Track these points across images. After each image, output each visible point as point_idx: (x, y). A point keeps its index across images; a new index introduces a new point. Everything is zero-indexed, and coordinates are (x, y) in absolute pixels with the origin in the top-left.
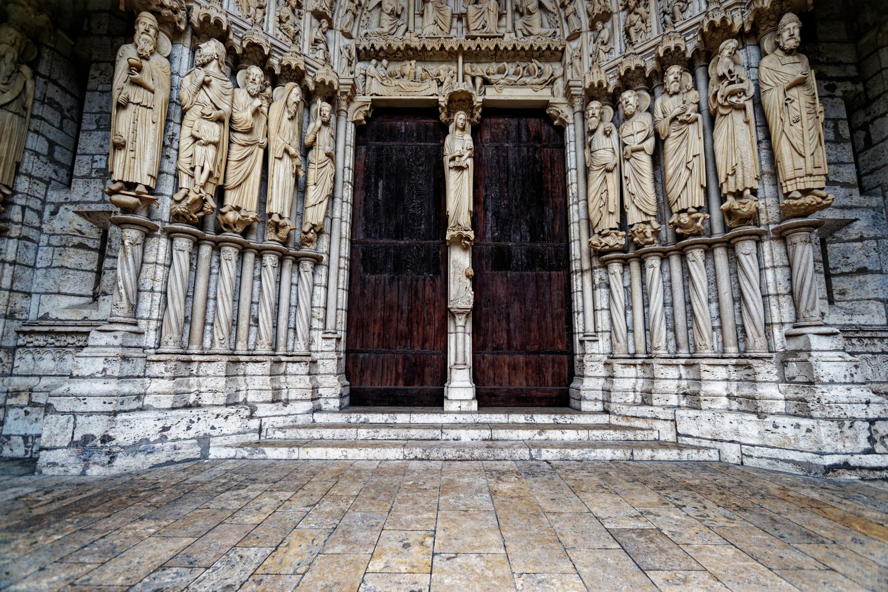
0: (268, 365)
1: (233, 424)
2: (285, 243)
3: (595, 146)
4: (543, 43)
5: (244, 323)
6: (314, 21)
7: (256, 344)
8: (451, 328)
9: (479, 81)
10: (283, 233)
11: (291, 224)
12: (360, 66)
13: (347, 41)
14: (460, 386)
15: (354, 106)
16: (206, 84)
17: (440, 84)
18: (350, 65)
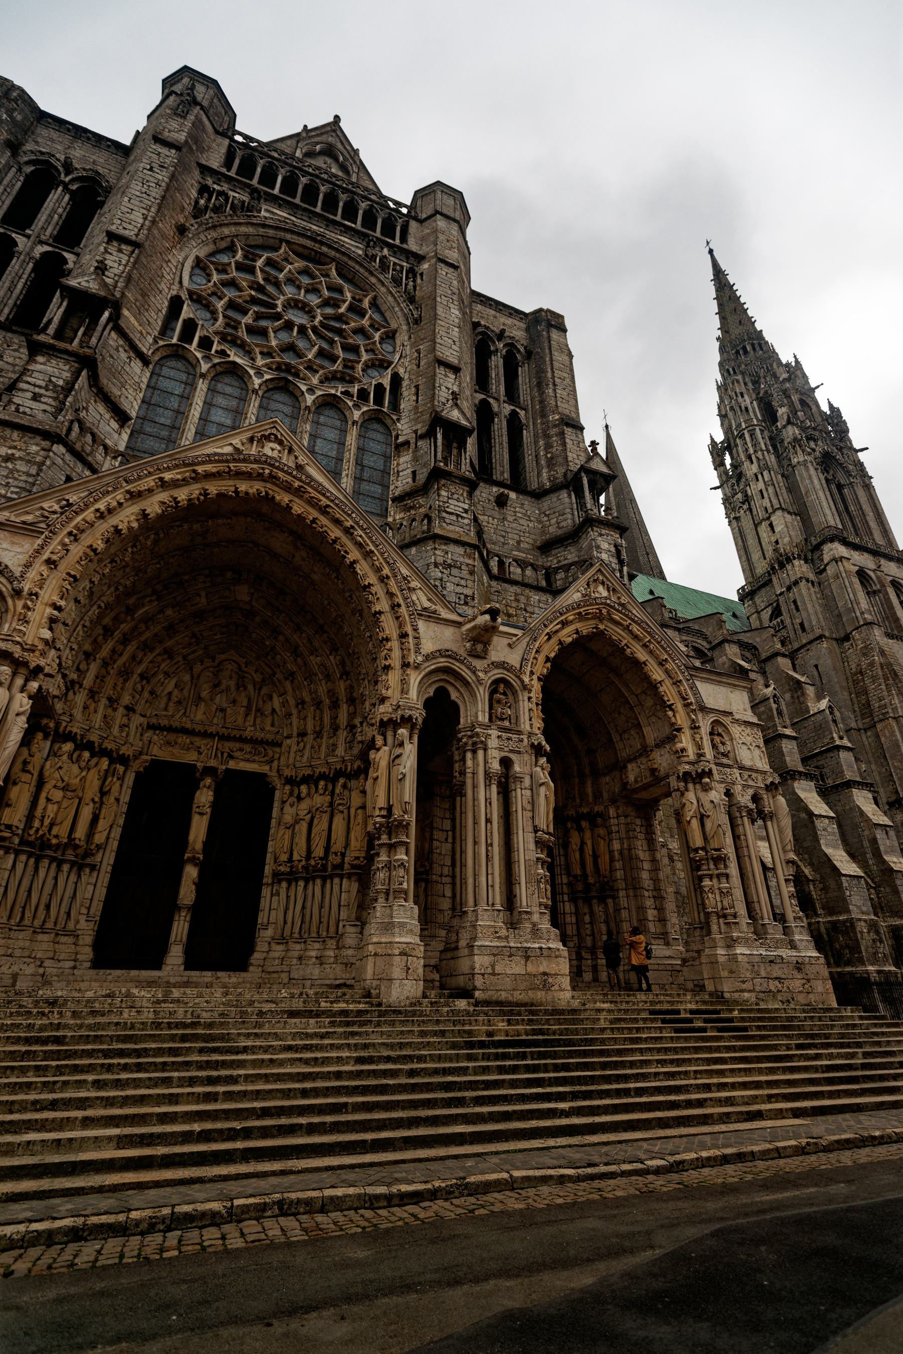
0: (53, 935)
1: (29, 970)
2: (76, 857)
3: (285, 810)
4: (270, 737)
5: (42, 907)
6: (125, 712)
7: (44, 922)
8: (176, 918)
9: (225, 755)
10: (78, 851)
11: (82, 843)
12: (148, 734)
13: (142, 719)
14: (176, 955)
15: (138, 761)
16: (60, 768)
17: (200, 753)
18: (142, 735)
